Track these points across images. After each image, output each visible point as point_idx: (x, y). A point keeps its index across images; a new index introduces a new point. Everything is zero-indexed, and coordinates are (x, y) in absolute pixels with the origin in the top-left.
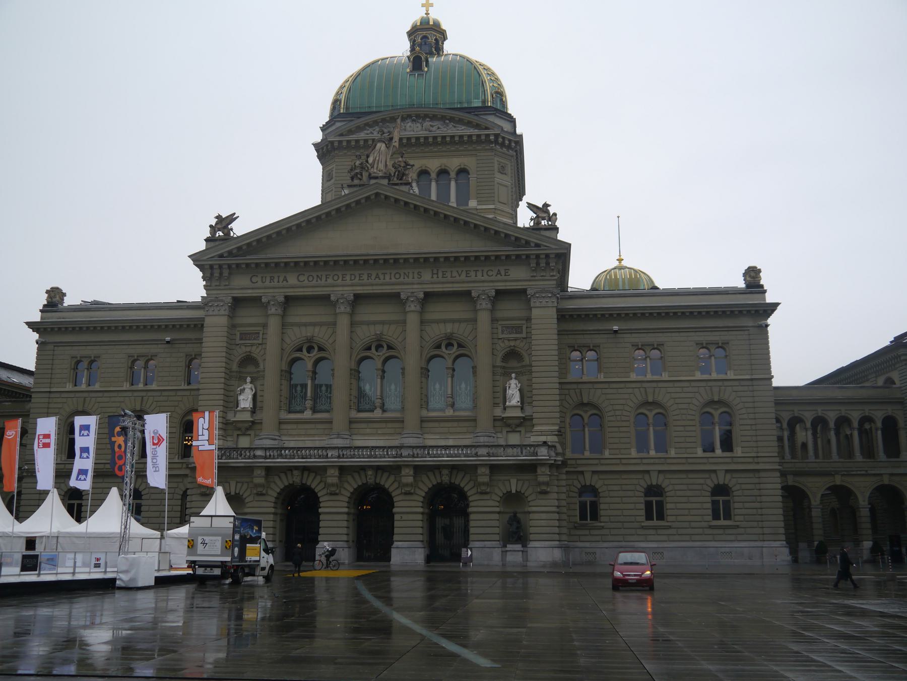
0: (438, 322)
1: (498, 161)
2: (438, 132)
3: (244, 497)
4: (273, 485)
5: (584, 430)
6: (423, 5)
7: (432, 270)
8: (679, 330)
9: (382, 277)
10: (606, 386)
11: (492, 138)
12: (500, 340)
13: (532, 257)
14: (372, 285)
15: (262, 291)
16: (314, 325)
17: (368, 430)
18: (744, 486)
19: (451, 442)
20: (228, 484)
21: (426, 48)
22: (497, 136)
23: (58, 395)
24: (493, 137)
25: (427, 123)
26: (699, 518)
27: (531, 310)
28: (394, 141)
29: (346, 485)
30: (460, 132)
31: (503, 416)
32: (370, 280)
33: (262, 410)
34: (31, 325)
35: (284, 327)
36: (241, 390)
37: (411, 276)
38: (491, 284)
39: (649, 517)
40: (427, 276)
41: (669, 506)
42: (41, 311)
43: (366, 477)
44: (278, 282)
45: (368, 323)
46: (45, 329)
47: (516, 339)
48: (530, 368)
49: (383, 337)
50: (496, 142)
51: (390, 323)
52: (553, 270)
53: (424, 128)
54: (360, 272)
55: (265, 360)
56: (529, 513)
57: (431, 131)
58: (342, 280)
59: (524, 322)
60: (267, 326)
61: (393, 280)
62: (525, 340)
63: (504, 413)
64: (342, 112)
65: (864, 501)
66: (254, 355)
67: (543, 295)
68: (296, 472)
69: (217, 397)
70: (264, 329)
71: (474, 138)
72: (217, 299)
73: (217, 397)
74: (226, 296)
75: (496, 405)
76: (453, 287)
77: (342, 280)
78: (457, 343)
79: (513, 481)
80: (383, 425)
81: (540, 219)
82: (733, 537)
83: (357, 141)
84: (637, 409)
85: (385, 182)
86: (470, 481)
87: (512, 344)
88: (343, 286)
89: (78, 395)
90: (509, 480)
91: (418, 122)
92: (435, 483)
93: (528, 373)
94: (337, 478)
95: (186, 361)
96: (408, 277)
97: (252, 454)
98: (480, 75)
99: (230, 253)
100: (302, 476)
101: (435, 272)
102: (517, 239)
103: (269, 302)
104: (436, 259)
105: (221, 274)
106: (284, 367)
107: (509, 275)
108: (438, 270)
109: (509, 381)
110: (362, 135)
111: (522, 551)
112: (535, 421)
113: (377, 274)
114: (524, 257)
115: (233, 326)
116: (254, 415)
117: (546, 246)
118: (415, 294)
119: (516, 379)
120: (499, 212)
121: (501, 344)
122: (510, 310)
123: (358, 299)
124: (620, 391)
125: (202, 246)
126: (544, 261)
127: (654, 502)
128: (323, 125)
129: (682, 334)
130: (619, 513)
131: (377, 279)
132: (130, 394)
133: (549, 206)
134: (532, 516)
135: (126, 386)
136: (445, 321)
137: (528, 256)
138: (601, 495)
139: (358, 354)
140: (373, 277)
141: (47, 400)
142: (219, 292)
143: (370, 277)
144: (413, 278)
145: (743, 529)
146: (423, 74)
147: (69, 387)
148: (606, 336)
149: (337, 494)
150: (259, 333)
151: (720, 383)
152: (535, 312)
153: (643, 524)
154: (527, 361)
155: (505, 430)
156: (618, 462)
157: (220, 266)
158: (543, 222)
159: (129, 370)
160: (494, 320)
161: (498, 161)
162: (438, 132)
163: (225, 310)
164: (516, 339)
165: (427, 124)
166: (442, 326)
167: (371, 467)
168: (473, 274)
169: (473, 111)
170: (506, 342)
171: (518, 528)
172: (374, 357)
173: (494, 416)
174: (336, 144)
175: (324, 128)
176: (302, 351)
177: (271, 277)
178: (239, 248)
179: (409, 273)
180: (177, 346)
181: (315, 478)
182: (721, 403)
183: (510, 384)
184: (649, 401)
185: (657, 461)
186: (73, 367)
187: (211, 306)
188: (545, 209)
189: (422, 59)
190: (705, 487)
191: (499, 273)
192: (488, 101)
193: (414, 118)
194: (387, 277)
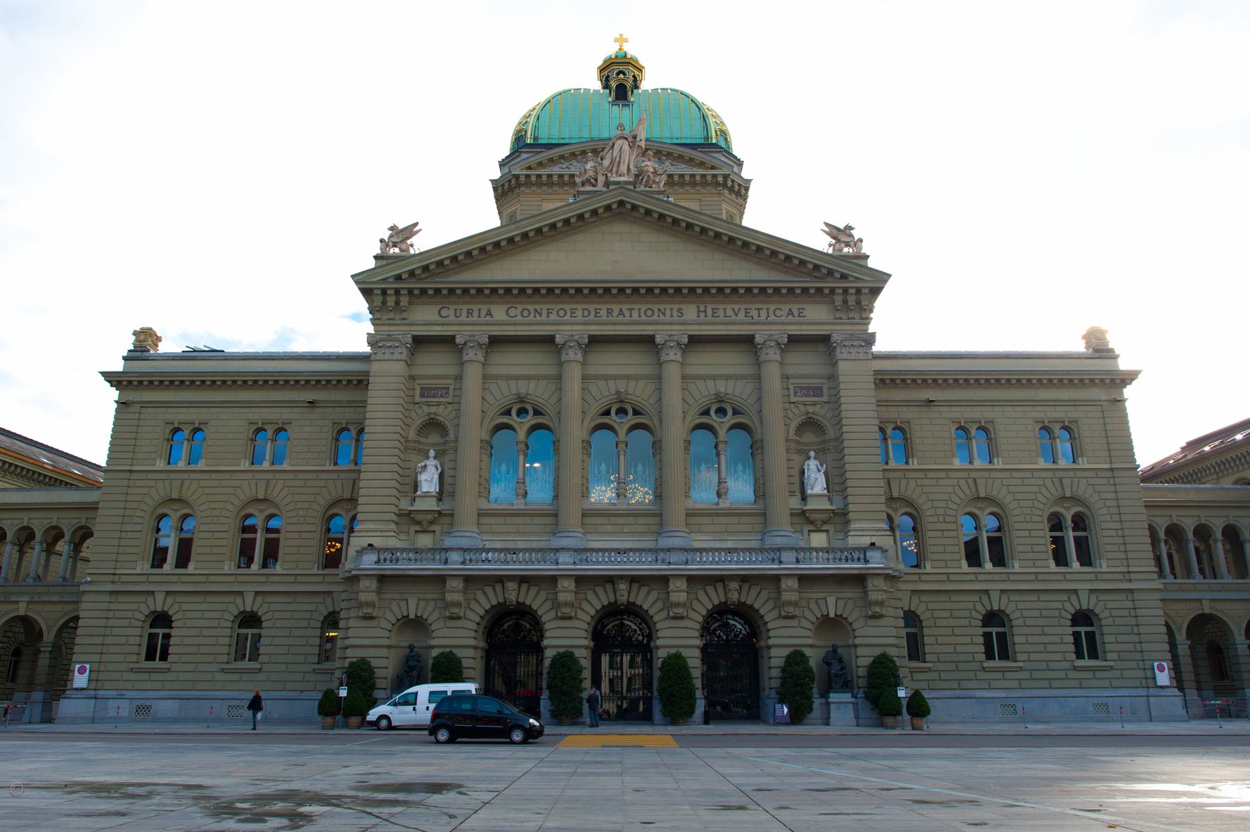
0: (705, 378)
1: (726, 209)
3: (429, 622)
4: (474, 605)
5: (894, 535)
6: (616, 40)
7: (698, 307)
8: (1013, 403)
9: (627, 313)
10: (922, 475)
11: (720, 179)
12: (793, 405)
13: (838, 291)
14: (615, 324)
15: (456, 328)
16: (528, 378)
17: (609, 527)
19: (729, 545)
20: (405, 603)
22: (726, 177)
23: (142, 476)
26: (1059, 657)
28: (638, 139)
29: (585, 606)
31: (805, 508)
32: (611, 318)
33: (454, 496)
34: (111, 377)
36: (422, 467)
37: (668, 312)
38: (781, 327)
39: (990, 655)
40: (690, 312)
41: (1017, 639)
42: (125, 358)
43: (615, 593)
44: (479, 317)
45: (606, 378)
46: (130, 382)
48: (835, 444)
49: (629, 397)
50: (725, 185)
51: (637, 378)
52: (865, 310)
56: (855, 646)
58: (571, 316)
59: (825, 381)
60: (461, 379)
61: (644, 318)
63: (806, 505)
64: (528, 141)
65: (1240, 635)
66: (442, 419)
67: (855, 344)
68: (511, 585)
69: (387, 476)
71: (698, 178)
72: (389, 337)
73: (387, 476)
74: (405, 333)
75: (792, 493)
77: (571, 316)
78: (733, 409)
79: (831, 600)
80: (631, 520)
81: (843, 245)
82: (1106, 683)
83: (550, 176)
85: (632, 187)
86: (767, 601)
87: (810, 409)
88: (572, 324)
89: (172, 476)
90: (825, 599)
92: (717, 602)
93: (834, 450)
94: (573, 594)
95: (333, 432)
96: (664, 315)
97: (444, 557)
98: (700, 110)
99: (412, 274)
100: (519, 591)
101: (702, 308)
102: (817, 267)
103: (465, 344)
104: (706, 290)
105: (397, 303)
106: (485, 436)
108: (706, 307)
109: (806, 461)
110: (556, 170)
111: (852, 703)
112: (851, 516)
113: (621, 310)
114: (826, 291)
115: (412, 378)
116: (441, 503)
117: (857, 278)
119: (815, 458)
121: (794, 410)
122: (806, 364)
123: (595, 341)
124: (940, 482)
125: (371, 264)
126: (854, 298)
127: (994, 634)
128: (503, 160)
129: (1016, 409)
130: (950, 649)
131: (621, 317)
132: (249, 476)
133: (853, 229)
134: (860, 651)
135: (245, 465)
136: (714, 378)
137: (832, 290)
138: (924, 624)
139: (592, 420)
140: (615, 313)
141: (125, 483)
142: (392, 328)
144: (672, 316)
145: (1119, 672)
146: (629, 105)
147: (160, 465)
148: (916, 409)
149: (570, 618)
150: (448, 388)
152: (842, 366)
153: (985, 665)
154: (831, 433)
155: (806, 528)
156: (945, 577)
157: (397, 292)
158: (846, 250)
159: (249, 442)
160: (786, 377)
161: (726, 209)
163: (401, 353)
166: (710, 383)
167: (622, 577)
168: (755, 313)
170: (801, 407)
171: (842, 669)
172: (615, 425)
173: (791, 509)
174: (522, 179)
176: (510, 415)
177: (468, 310)
178: (426, 268)
179: (665, 309)
180: (320, 410)
181: (538, 592)
182: (1074, 499)
183: (808, 465)
184: (981, 496)
185: (996, 577)
186: (166, 436)
187: (380, 347)
188: (848, 231)
190: (1064, 614)
191: (791, 312)
192: (711, 138)
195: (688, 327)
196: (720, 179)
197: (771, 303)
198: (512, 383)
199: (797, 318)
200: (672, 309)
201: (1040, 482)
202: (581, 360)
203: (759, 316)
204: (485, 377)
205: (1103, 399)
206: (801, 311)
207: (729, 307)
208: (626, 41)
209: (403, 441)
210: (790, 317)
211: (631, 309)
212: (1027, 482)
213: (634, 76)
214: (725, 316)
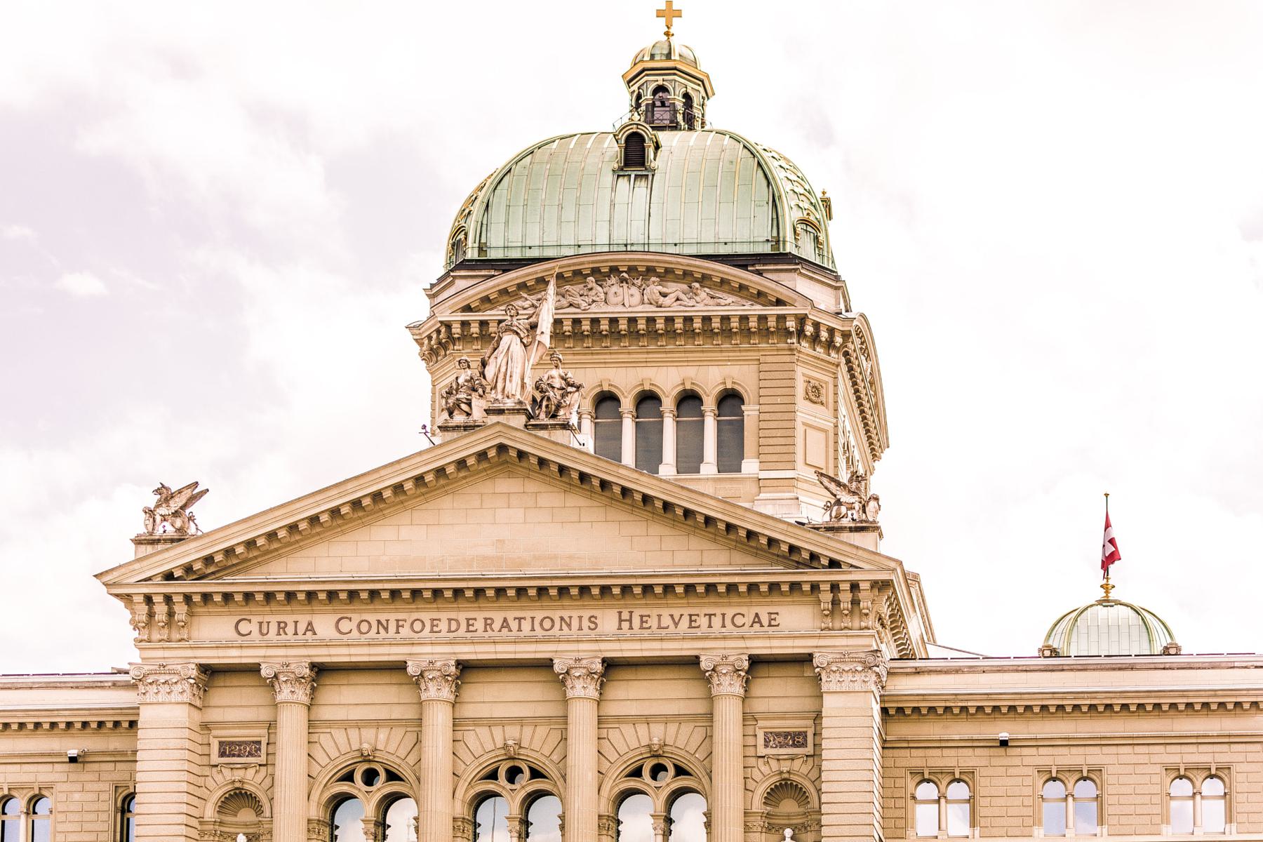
2: (676, 307)
7: (620, 613)
13: (823, 587)
16: (377, 724)
21: (662, 115)
25: (652, 286)
27: (822, 696)
30: (717, 311)
32: (490, 633)
35: (310, 731)
37: (575, 624)
38: (741, 644)
47: (792, 758)
52: (867, 615)
53: (645, 298)
54: (471, 615)
55: (273, 798)
57: (661, 307)
61: (539, 632)
62: (810, 760)
67: (847, 669)
70: (269, 733)
76: (662, 649)
81: (843, 510)
91: (633, 284)
96: (569, 626)
101: (625, 616)
102: (793, 549)
107: (778, 625)
113: (505, 620)
114: (806, 588)
117: (852, 566)
118: (584, 662)
131: (505, 630)
137: (815, 587)
140: (497, 626)
143: (491, 625)
150: (259, 743)
160: (748, 718)
162: (676, 307)
164: (792, 758)
165: (654, 288)
168: (703, 621)
169: (751, 263)
175: (435, 290)
179: (570, 617)
180: (96, 766)
189: (644, 140)
193: (625, 275)
194: (526, 626)
195: (603, 646)
197: (730, 605)
198: (353, 733)
199: (766, 628)
200: (580, 617)
202: (452, 698)
203: (710, 626)
204: (312, 724)
206: (773, 616)
207: (665, 613)
208: (678, 14)
209: (195, 823)
210: (757, 626)
211: (520, 619)
213: (687, 96)
214: (660, 627)
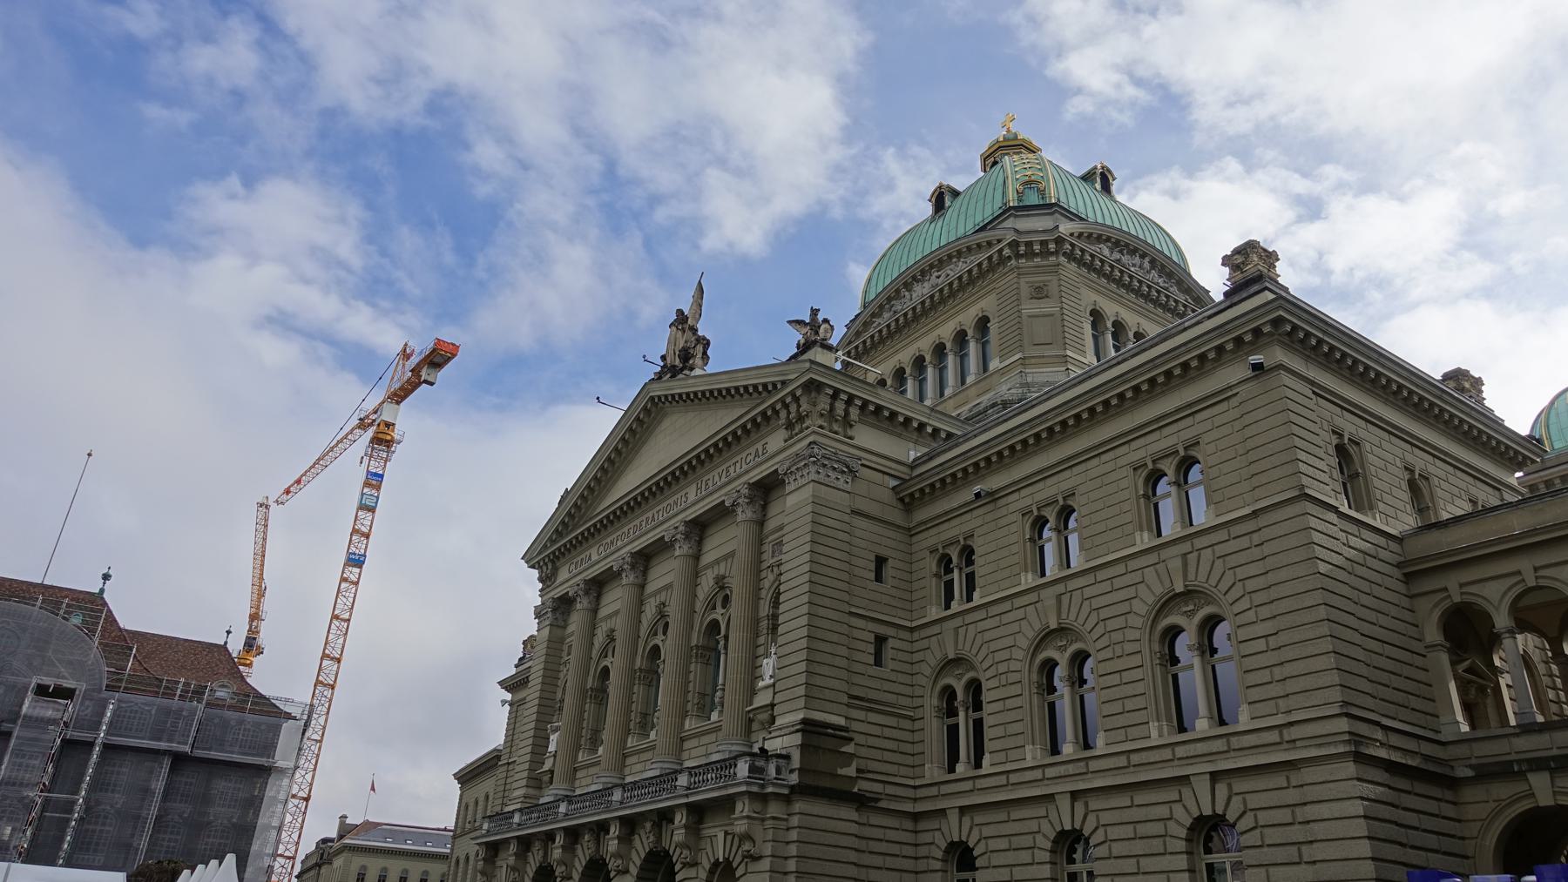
1: (1027, 283)
8: (1096, 451)
11: (1007, 252)
18: (1264, 818)
22: (1014, 245)
24: (1008, 251)
50: (1018, 256)
84: (1034, 655)
102: (765, 386)
120: (1033, 361)
129: (1105, 458)
151: (1186, 547)
196: (1007, 252)
201: (1137, 577)
205: (1233, 381)
212: (1118, 583)
